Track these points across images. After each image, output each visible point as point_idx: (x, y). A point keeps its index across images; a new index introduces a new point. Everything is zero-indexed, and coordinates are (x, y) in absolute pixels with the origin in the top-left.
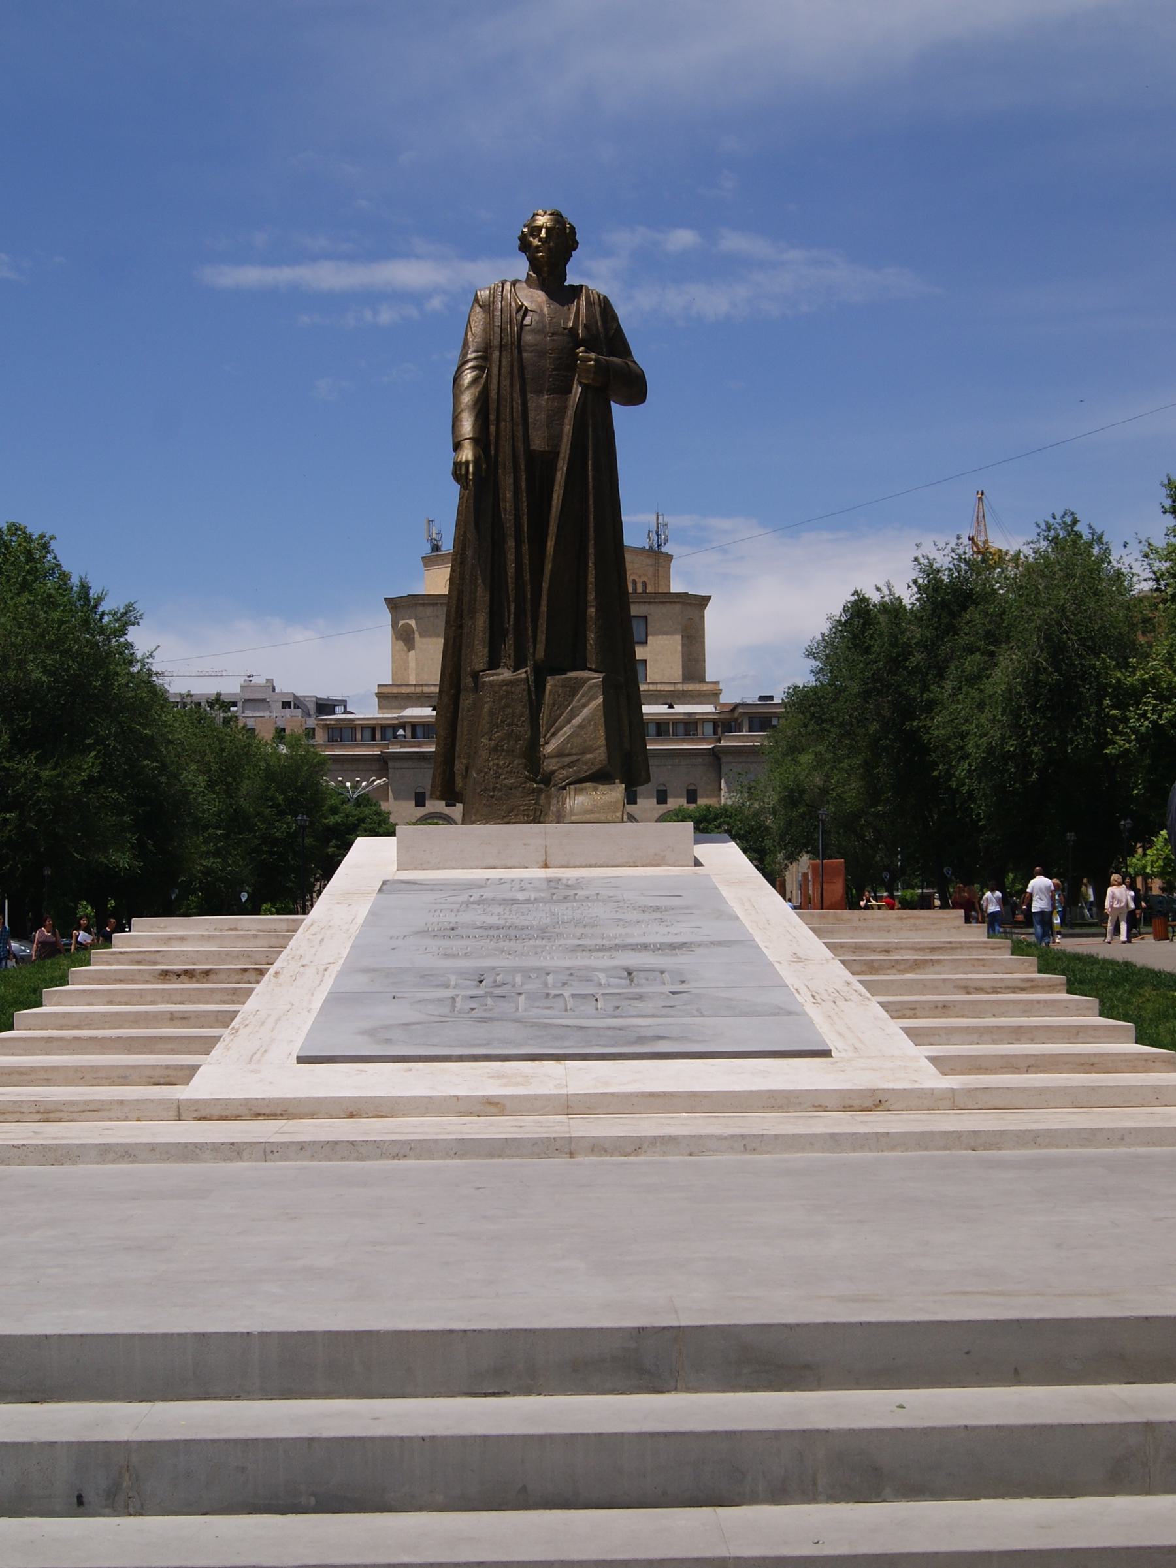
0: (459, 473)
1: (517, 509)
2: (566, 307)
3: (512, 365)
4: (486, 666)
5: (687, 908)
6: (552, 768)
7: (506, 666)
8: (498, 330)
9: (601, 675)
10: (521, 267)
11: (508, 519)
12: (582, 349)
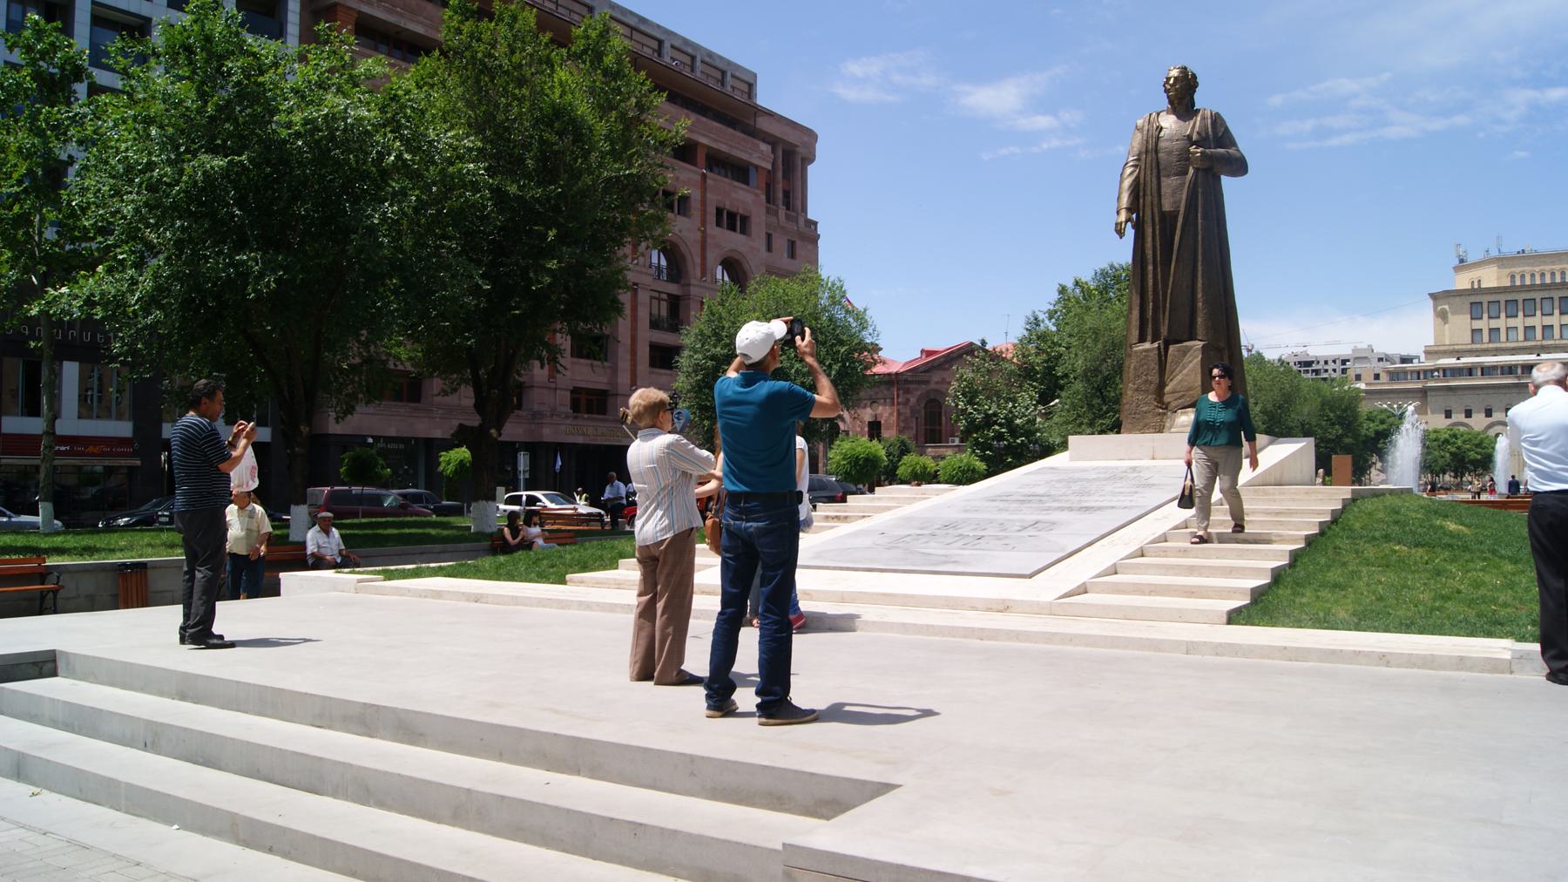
11: (1149, 253)
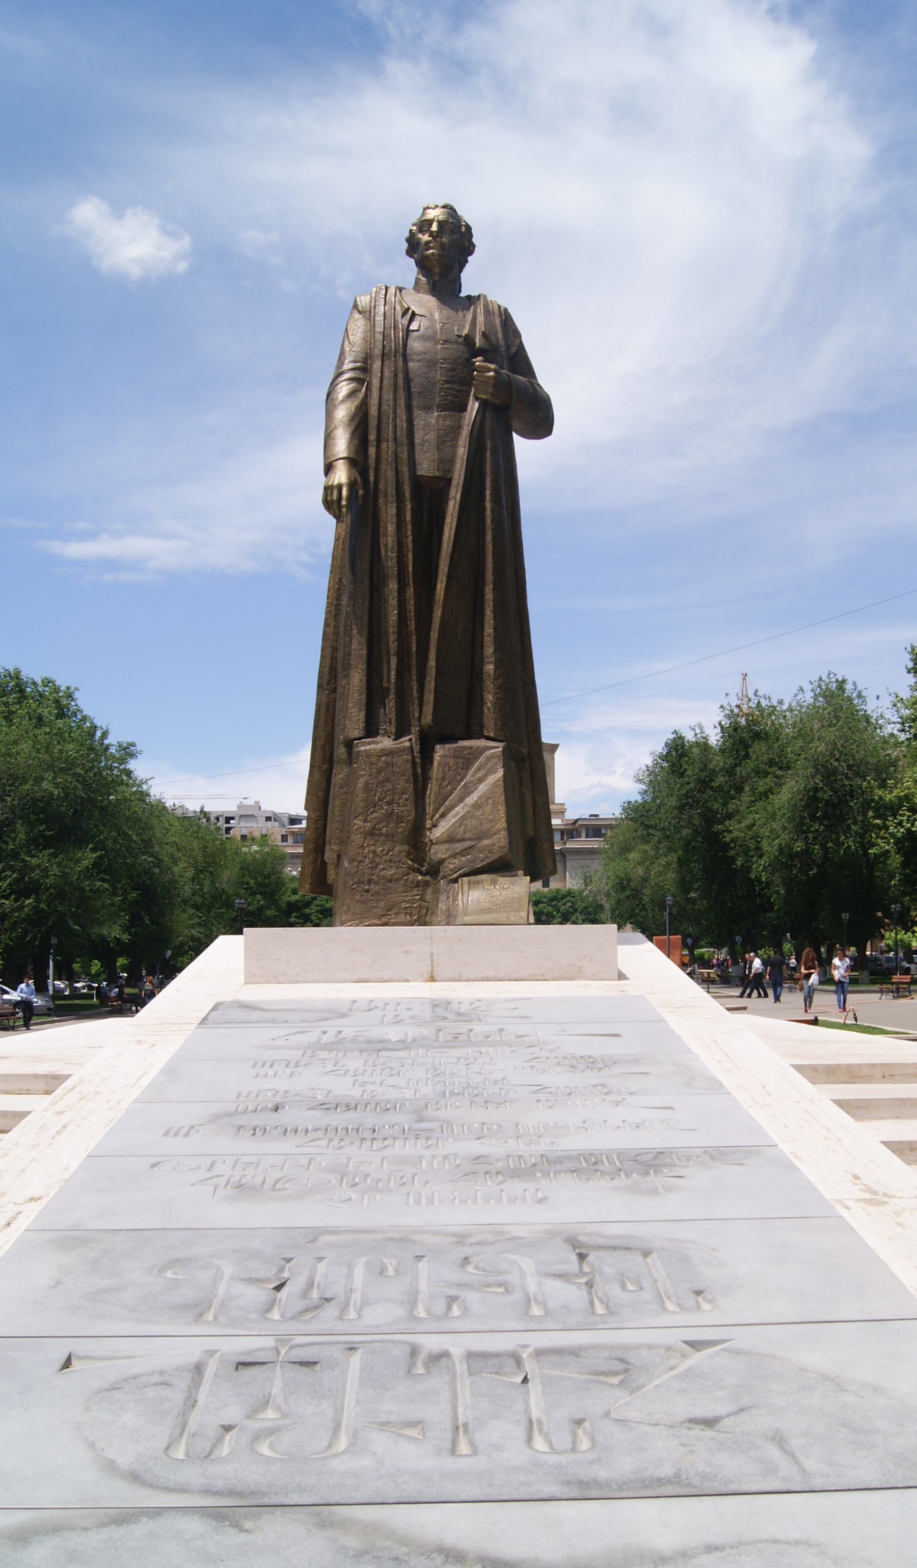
0: (331, 503)
1: (401, 545)
2: (460, 313)
3: (396, 376)
4: (362, 733)
5: (635, 1061)
6: (440, 856)
7: (386, 734)
8: (379, 337)
9: (501, 744)
10: (407, 271)
11: (390, 557)
12: (478, 359)
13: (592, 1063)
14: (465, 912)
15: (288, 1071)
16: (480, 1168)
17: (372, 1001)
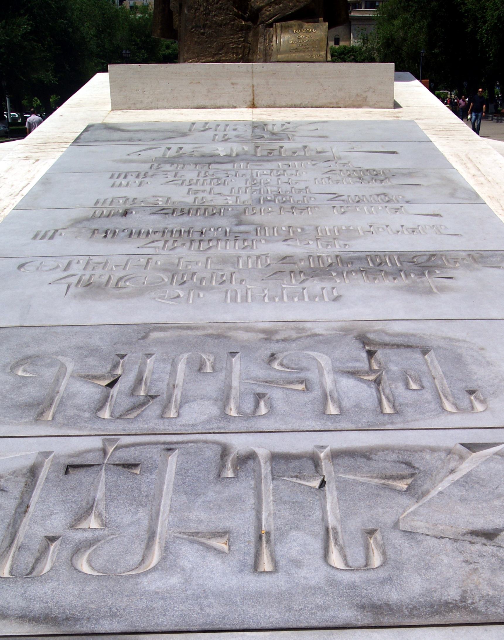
13: (376, 176)
14: (278, 52)
15: (138, 181)
16: (287, 268)
17: (206, 123)
